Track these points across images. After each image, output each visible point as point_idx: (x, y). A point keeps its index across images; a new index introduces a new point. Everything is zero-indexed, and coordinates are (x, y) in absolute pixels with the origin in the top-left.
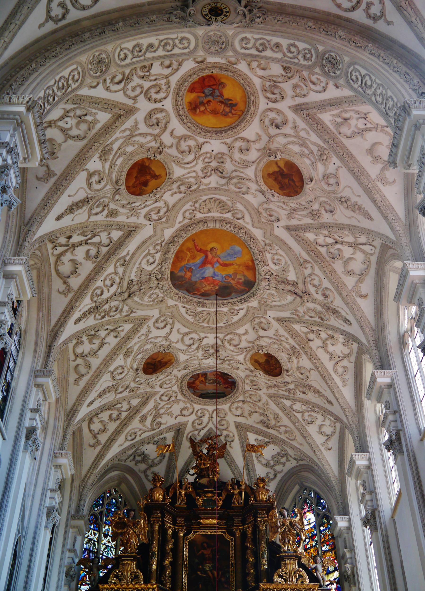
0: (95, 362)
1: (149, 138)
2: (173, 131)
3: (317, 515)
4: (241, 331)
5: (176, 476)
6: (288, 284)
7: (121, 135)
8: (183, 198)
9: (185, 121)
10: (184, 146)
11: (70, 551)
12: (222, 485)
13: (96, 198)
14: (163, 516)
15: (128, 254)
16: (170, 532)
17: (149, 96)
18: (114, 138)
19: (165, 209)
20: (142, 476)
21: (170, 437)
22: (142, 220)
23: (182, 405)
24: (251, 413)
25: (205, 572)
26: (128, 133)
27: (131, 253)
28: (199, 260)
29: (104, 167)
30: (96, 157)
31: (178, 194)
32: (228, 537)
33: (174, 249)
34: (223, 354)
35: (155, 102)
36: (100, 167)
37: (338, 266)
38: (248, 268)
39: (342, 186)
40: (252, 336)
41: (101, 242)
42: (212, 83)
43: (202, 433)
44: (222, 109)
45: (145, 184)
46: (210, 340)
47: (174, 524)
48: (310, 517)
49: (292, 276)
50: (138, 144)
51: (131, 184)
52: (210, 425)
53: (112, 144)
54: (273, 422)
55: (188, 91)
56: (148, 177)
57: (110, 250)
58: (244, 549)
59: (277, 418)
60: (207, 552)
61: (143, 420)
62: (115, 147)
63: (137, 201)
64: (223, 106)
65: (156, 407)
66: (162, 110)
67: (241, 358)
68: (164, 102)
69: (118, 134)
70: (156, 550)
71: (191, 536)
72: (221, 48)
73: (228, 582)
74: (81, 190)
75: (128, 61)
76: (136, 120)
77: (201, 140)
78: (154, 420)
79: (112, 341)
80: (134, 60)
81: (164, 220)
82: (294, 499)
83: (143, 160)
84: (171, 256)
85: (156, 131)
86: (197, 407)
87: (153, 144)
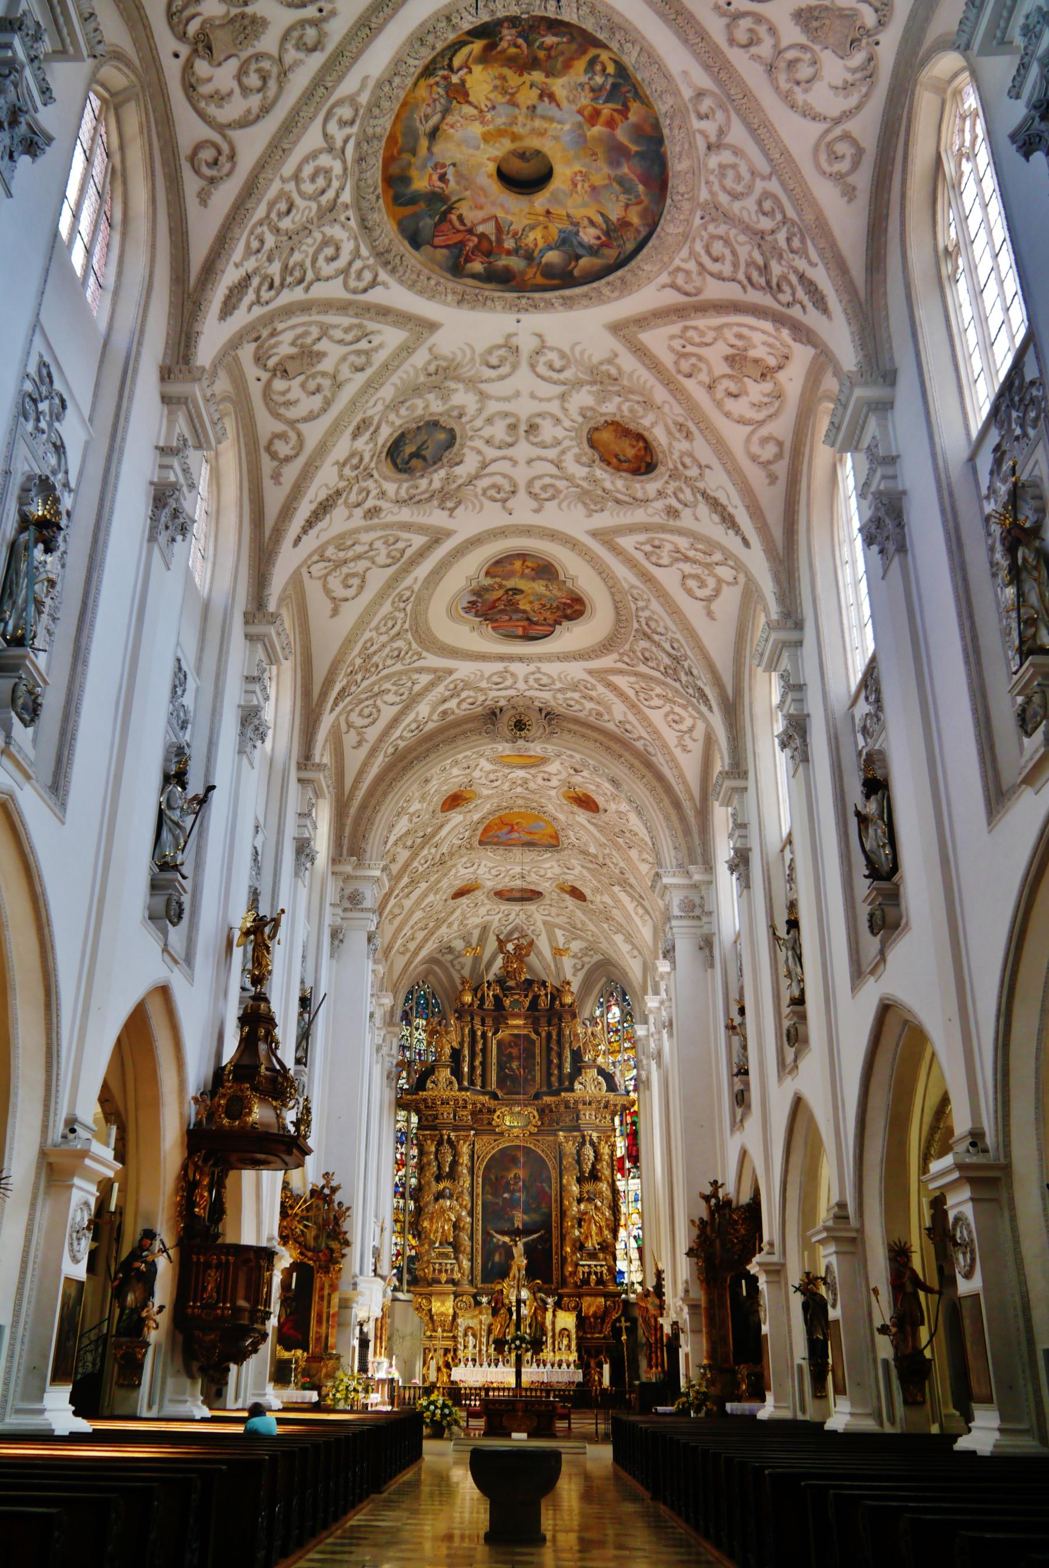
0: (408, 903)
3: (622, 1011)
4: (547, 865)
5: (483, 966)
6: (589, 854)
10: (492, 777)
11: (390, 1055)
12: (529, 983)
14: (472, 1019)
16: (479, 1033)
20: (449, 965)
21: (476, 933)
23: (488, 907)
24: (558, 915)
25: (512, 1070)
28: (506, 829)
32: (534, 1036)
33: (481, 828)
34: (528, 879)
37: (634, 854)
38: (551, 837)
39: (631, 823)
40: (557, 870)
43: (509, 928)
46: (518, 869)
47: (483, 1025)
48: (615, 1011)
49: (592, 850)
52: (517, 921)
54: (579, 926)
58: (549, 1050)
59: (583, 923)
60: (515, 1051)
61: (449, 926)
65: (463, 914)
67: (547, 884)
70: (466, 1052)
71: (500, 1035)
73: (534, 1080)
78: (461, 923)
79: (424, 885)
82: (601, 990)
84: (479, 832)
86: (503, 908)
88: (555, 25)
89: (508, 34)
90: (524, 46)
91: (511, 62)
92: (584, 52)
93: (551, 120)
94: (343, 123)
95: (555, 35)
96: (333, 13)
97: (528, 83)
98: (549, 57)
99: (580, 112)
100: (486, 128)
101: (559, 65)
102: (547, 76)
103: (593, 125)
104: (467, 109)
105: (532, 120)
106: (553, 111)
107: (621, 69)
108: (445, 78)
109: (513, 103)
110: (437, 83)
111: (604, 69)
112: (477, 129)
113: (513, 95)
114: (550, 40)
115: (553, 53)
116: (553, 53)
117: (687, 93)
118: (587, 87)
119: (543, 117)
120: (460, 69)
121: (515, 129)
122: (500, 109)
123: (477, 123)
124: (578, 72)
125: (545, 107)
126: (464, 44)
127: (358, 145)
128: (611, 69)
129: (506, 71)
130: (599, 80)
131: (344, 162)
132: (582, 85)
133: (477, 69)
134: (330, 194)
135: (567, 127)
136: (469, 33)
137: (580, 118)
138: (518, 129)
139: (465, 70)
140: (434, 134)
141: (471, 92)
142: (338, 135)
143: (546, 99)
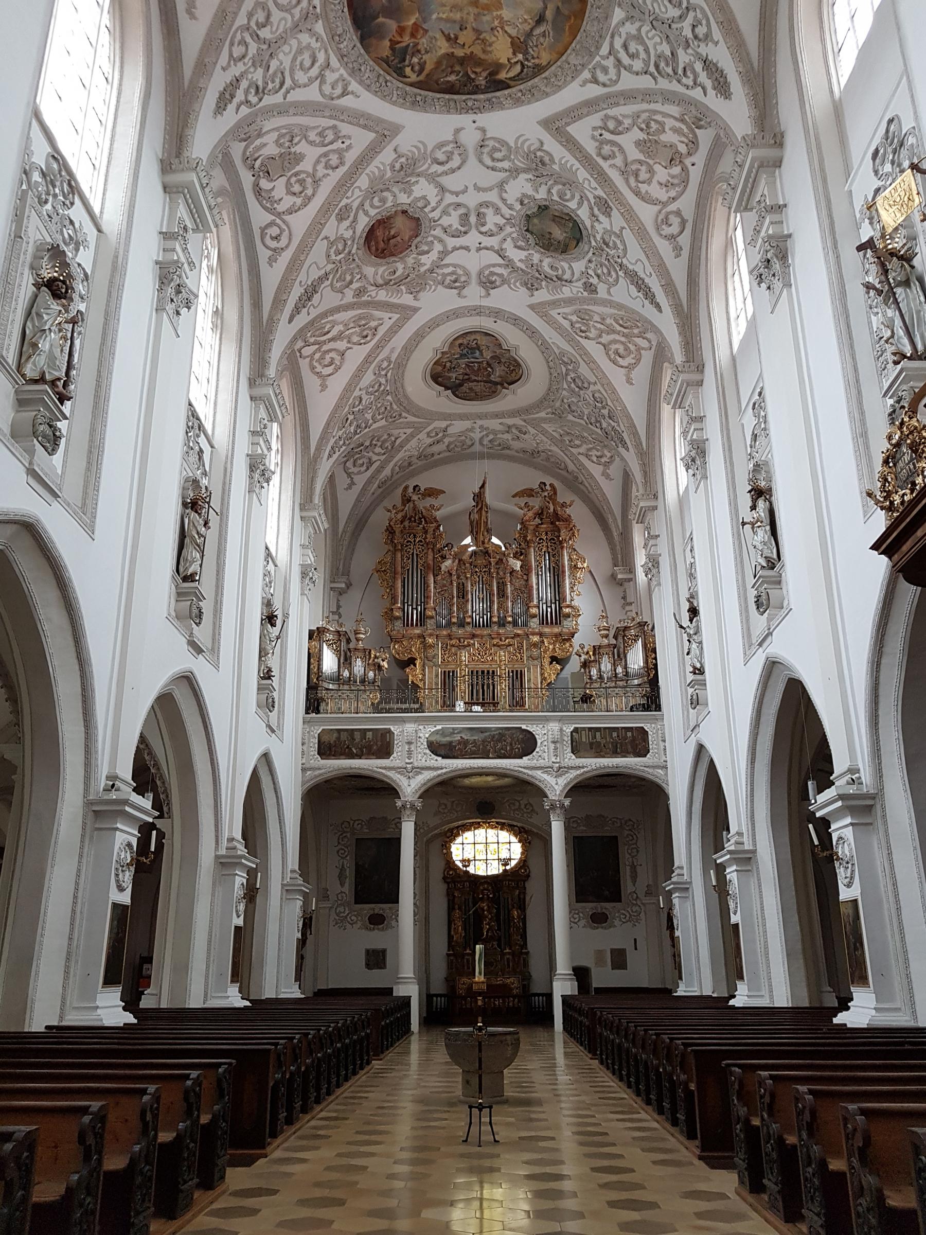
88: (451, 89)
89: (481, 81)
90: (470, 72)
91: (479, 62)
92: (428, 75)
93: (447, 20)
94: (605, 70)
95: (448, 82)
96: (595, 129)
97: (466, 47)
98: (452, 67)
99: (426, 31)
100: (499, 13)
101: (445, 62)
102: (453, 53)
103: (415, 24)
104: (513, 32)
105: (462, 18)
106: (447, 28)
107: (400, 73)
108: (527, 60)
109: (478, 32)
110: (533, 58)
111: (412, 69)
112: (506, 14)
113: (478, 39)
114: (452, 78)
115: (449, 69)
116: (449, 69)
117: (354, 86)
118: (423, 52)
119: (455, 22)
120: (517, 62)
121: (476, 11)
122: (488, 28)
123: (505, 19)
124: (430, 61)
125: (452, 31)
126: (510, 79)
127: (598, 48)
128: (408, 70)
129: (483, 56)
130: (415, 60)
131: (612, 45)
132: (427, 52)
133: (504, 60)
134: (630, 28)
135: (434, 16)
136: (509, 87)
137: (424, 26)
138: (473, 10)
139: (512, 61)
140: (541, 20)
141: (509, 45)
142: (610, 63)
143: (452, 36)
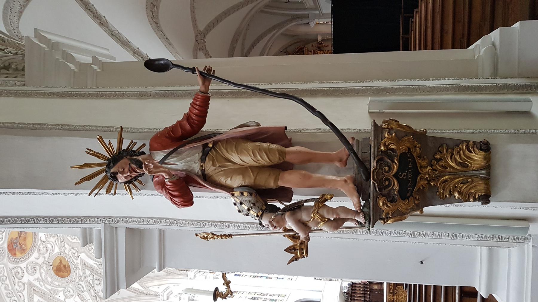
1: (42, 270)
2: (36, 258)
7: (43, 286)
8: (67, 244)
9: (31, 254)
13: (77, 291)
15: (96, 264)
17: (21, 277)
18: (45, 290)
19: (72, 250)
22: (79, 261)
26: (41, 283)
27: (95, 262)
29: (61, 291)
30: (57, 296)
31: (65, 246)
35: (24, 273)
36: (62, 293)
41: (92, 279)
42: (11, 245)
44: (23, 236)
45: (65, 266)
50: (46, 276)
51: (66, 274)
53: (49, 290)
55: (16, 256)
56: (62, 266)
57: (95, 274)
62: (50, 287)
63: (72, 267)
64: (21, 236)
66: (27, 268)
68: (23, 268)
69: (43, 288)
72: (2, 251)
74: (75, 299)
75: (16, 299)
76: (33, 280)
77: (40, 242)
80: (14, 295)
81: (77, 249)
83: (54, 271)
85: (38, 267)
87: (45, 267)
